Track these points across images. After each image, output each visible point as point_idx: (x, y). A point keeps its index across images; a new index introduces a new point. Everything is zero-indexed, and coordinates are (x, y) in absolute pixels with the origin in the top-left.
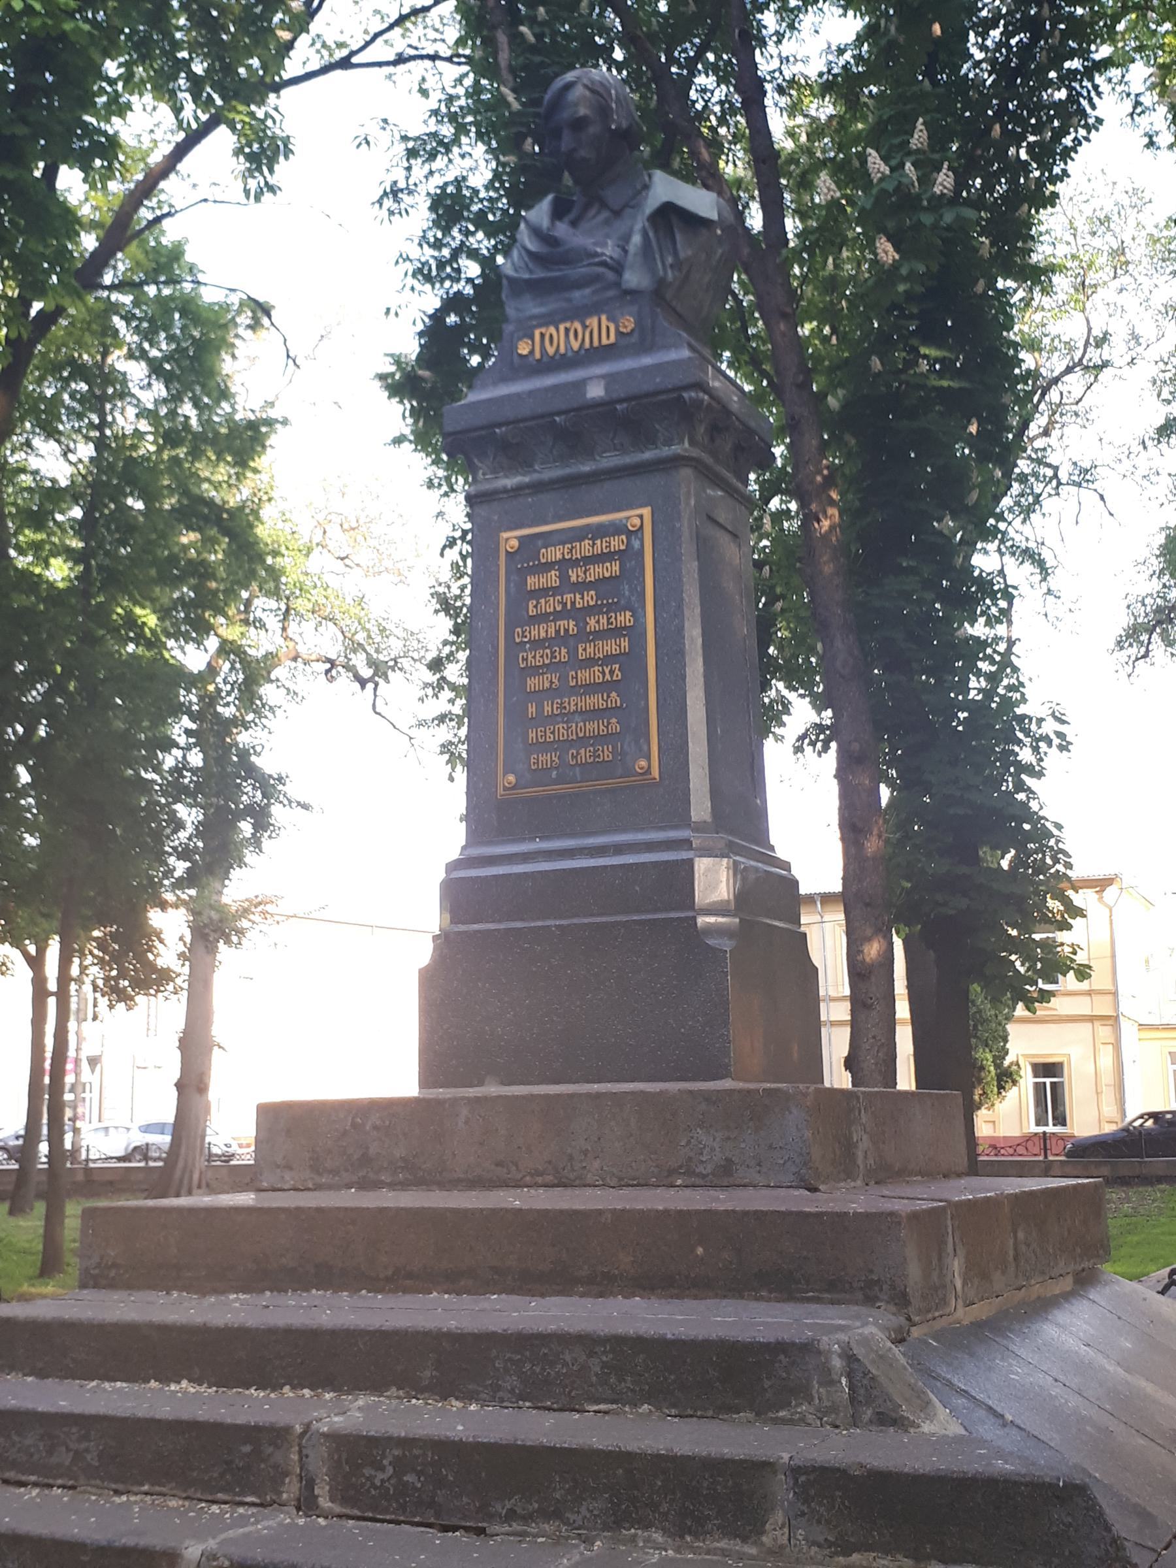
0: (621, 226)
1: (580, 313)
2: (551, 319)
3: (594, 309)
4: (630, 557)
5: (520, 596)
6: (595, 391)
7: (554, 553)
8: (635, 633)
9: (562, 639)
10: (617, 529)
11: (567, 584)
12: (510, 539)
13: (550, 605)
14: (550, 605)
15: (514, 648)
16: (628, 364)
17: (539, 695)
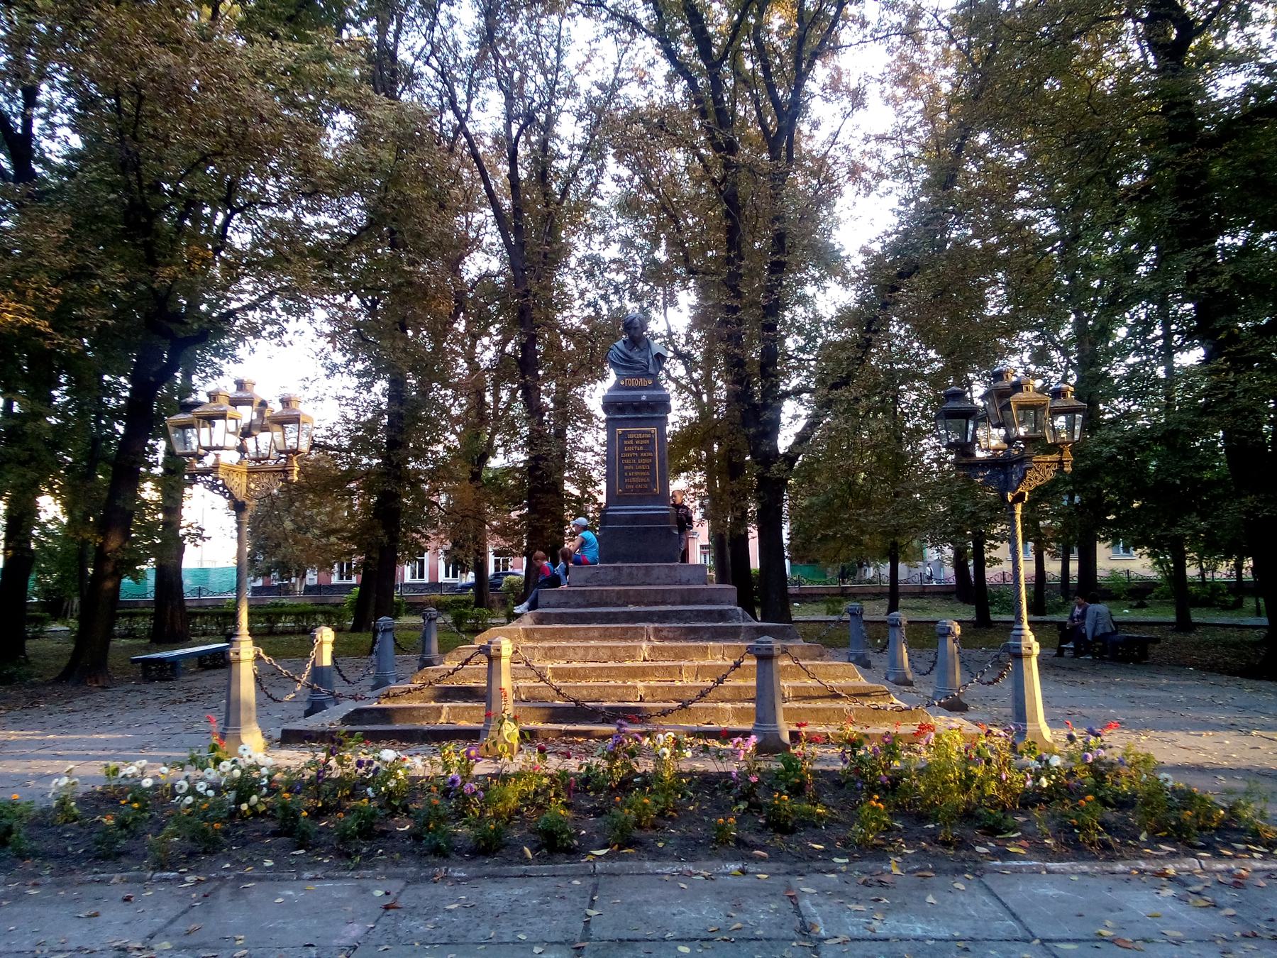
0: (644, 354)
1: (638, 377)
2: (630, 377)
3: (642, 376)
4: (652, 440)
5: (622, 447)
6: (644, 398)
7: (630, 436)
8: (653, 458)
9: (634, 457)
10: (649, 432)
11: (635, 444)
12: (620, 430)
13: (630, 449)
14: (630, 449)
15: (620, 459)
16: (651, 393)
17: (628, 471)
